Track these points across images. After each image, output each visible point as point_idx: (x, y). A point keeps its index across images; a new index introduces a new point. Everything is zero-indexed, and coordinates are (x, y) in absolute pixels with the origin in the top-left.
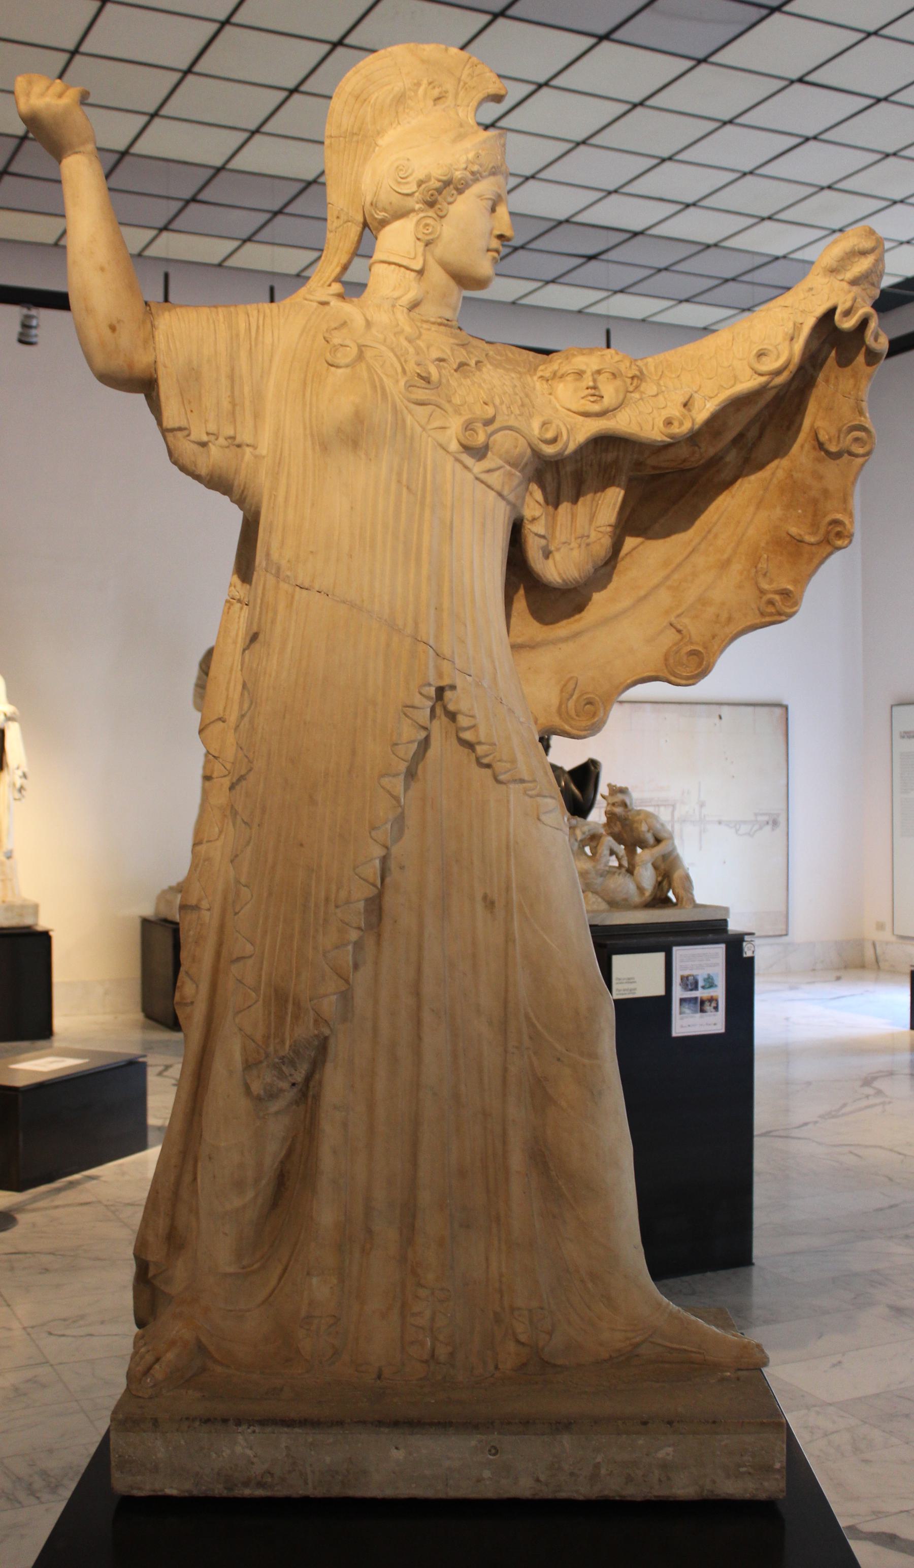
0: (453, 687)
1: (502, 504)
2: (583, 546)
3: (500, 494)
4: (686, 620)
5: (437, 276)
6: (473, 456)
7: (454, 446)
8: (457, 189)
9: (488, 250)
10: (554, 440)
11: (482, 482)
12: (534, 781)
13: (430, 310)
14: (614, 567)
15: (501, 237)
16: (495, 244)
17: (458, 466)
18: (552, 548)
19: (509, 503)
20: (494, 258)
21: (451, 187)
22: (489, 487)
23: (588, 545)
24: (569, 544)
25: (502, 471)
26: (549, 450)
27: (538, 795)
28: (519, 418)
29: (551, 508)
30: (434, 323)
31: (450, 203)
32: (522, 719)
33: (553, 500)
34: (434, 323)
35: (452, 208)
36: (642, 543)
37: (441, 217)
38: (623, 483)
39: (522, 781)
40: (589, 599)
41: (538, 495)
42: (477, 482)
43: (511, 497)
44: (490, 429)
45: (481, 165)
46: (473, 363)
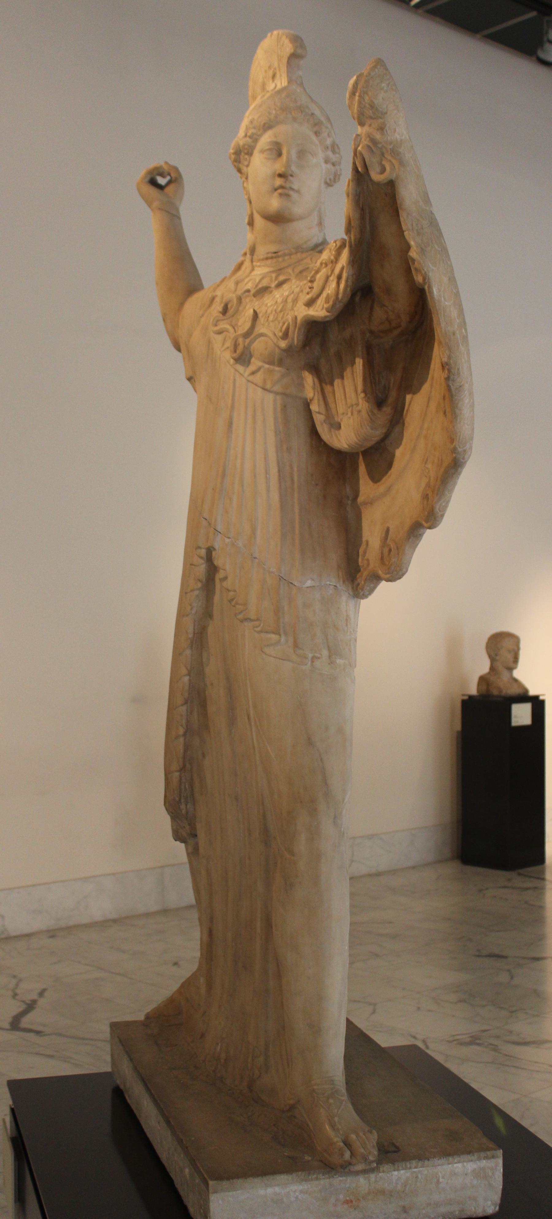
0: (215, 549)
1: (271, 397)
2: (355, 413)
3: (264, 389)
4: (429, 466)
5: (259, 221)
6: (242, 365)
7: (232, 361)
8: (247, 154)
9: (276, 190)
10: (285, 335)
11: (252, 383)
12: (258, 620)
13: (261, 251)
14: (404, 424)
15: (280, 176)
16: (279, 182)
17: (237, 375)
18: (339, 420)
19: (276, 393)
20: (281, 195)
21: (243, 154)
22: (256, 385)
23: (359, 411)
24: (347, 414)
25: (262, 370)
26: (283, 344)
27: (261, 631)
28: (271, 324)
29: (328, 388)
30: (263, 260)
31: (247, 166)
32: (273, 570)
33: (325, 379)
34: (263, 260)
35: (249, 168)
36: (412, 398)
37: (247, 178)
38: (360, 353)
39: (251, 620)
40: (393, 456)
41: (309, 379)
42: (250, 384)
43: (278, 388)
44: (248, 341)
45: (254, 128)
46: (273, 285)
